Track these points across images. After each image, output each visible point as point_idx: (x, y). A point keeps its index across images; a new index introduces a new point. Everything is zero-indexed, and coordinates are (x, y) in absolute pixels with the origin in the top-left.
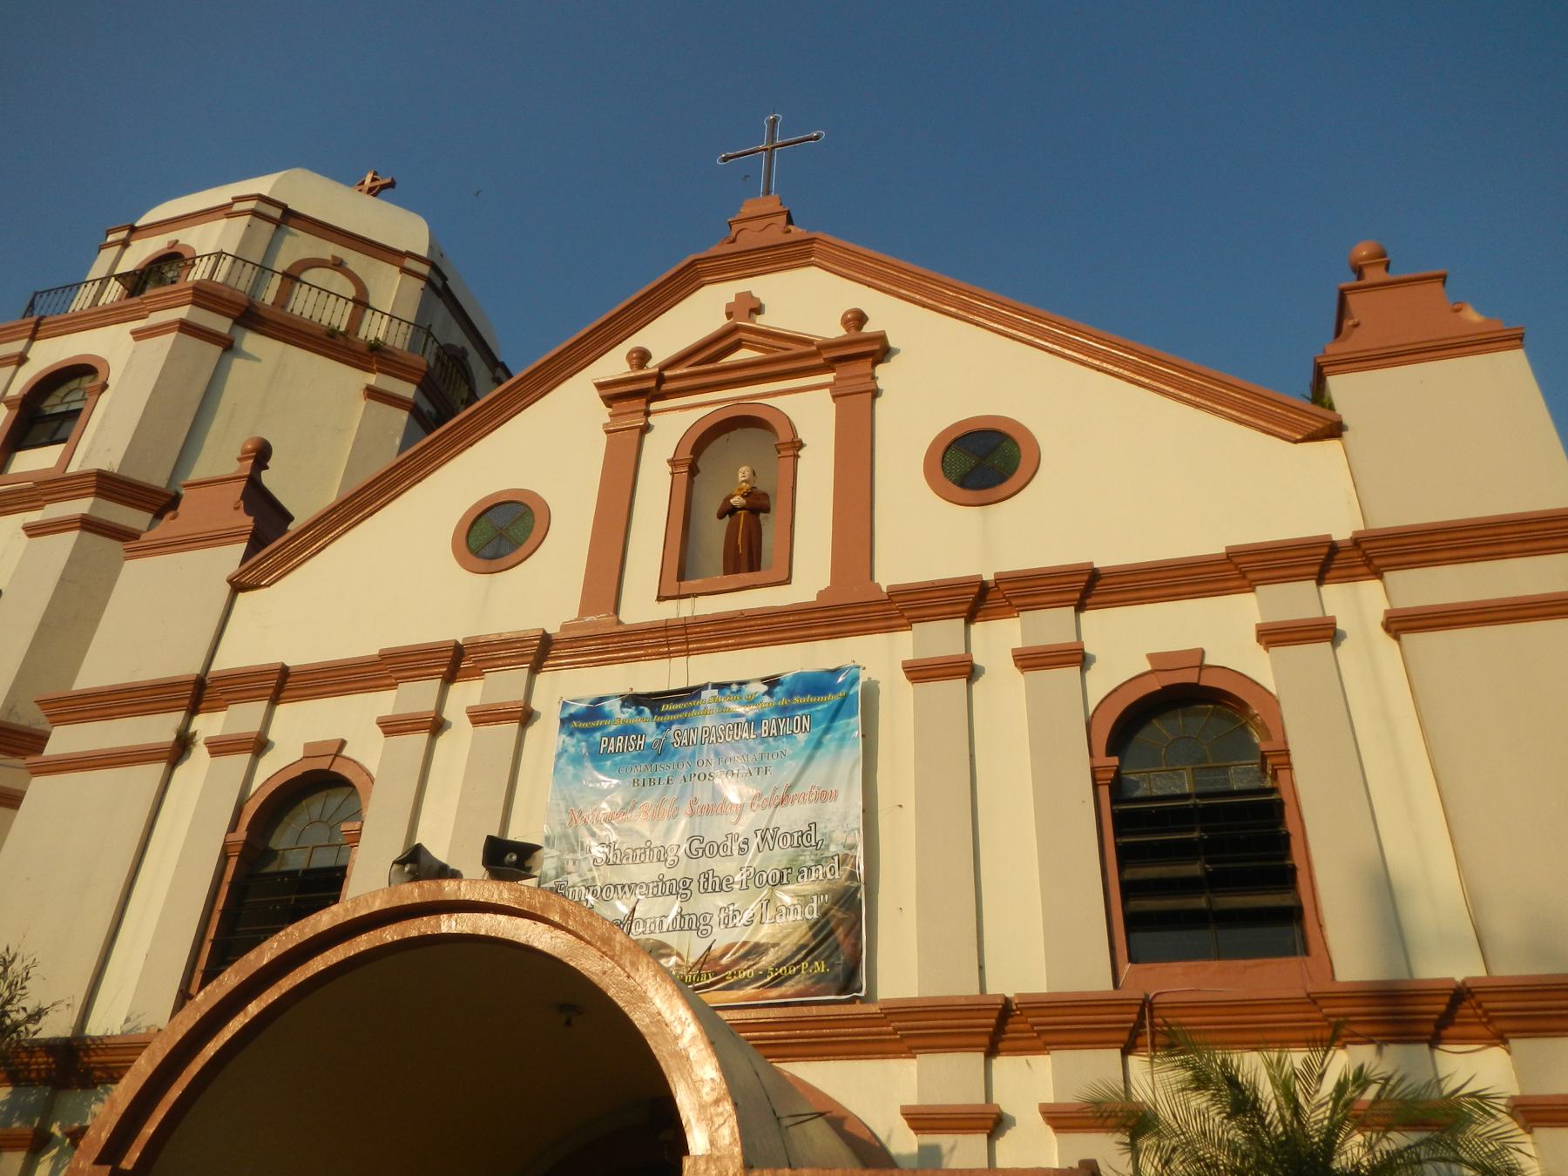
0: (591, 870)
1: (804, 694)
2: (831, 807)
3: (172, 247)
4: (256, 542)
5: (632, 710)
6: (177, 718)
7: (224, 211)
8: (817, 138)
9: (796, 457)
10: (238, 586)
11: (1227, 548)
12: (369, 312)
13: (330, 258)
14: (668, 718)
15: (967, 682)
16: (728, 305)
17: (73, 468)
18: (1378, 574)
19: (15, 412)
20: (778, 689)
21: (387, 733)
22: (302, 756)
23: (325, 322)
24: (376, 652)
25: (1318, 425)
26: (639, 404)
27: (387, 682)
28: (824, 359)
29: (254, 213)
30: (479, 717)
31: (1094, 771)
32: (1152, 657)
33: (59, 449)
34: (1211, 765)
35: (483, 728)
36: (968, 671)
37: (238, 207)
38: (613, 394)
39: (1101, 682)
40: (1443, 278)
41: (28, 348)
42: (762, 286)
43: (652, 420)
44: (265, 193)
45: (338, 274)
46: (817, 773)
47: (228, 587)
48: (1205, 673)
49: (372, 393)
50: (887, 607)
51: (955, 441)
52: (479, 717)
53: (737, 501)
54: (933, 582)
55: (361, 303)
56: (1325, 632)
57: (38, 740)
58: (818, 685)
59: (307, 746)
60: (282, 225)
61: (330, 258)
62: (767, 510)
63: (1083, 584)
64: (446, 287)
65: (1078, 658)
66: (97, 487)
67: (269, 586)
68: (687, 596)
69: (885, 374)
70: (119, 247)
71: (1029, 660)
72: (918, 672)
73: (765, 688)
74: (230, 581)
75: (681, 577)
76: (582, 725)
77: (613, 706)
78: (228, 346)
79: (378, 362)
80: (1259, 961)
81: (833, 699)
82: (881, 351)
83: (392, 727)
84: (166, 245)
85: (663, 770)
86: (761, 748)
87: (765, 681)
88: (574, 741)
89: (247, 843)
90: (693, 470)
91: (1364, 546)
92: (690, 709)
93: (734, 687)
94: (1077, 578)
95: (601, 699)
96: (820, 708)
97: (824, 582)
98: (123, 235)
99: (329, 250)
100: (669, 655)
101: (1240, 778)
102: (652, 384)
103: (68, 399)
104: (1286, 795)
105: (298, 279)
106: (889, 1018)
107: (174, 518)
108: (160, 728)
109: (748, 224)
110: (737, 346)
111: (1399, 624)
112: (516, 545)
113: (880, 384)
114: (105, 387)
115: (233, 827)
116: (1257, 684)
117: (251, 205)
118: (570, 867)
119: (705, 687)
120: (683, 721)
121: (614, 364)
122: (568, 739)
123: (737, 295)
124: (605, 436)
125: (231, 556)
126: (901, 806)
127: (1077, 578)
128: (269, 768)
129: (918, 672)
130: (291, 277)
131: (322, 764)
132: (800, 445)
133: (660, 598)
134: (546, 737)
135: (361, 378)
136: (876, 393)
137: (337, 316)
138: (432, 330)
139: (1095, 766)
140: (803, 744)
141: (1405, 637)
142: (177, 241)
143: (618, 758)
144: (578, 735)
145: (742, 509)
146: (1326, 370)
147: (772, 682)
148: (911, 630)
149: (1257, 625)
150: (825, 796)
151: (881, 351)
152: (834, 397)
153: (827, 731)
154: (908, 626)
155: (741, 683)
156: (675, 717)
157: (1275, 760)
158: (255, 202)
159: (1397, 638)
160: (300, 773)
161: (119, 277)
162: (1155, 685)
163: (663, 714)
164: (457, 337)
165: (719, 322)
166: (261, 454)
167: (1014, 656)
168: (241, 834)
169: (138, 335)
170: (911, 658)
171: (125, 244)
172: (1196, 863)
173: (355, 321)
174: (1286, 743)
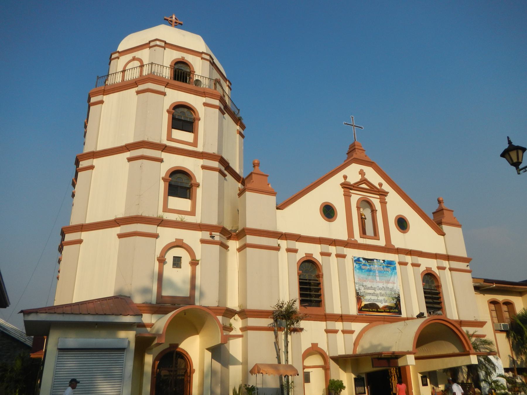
0: (364, 290)
1: (389, 264)
2: (395, 285)
5: (364, 261)
8: (362, 128)
14: (370, 264)
18: (448, 261)
20: (385, 262)
32: (426, 267)
37: (204, 56)
40: (453, 211)
46: (392, 279)
58: (390, 263)
66: (220, 160)
73: (383, 262)
76: (358, 262)
77: (361, 259)
79: (240, 123)
81: (393, 266)
83: (322, 254)
85: (371, 273)
86: (385, 273)
87: (383, 260)
88: (357, 265)
92: (373, 263)
93: (378, 260)
95: (359, 258)
96: (391, 267)
100: (364, 250)
109: (359, 150)
111: (451, 269)
114: (199, 119)
118: (360, 289)
119: (374, 259)
120: (372, 265)
133: (361, 237)
134: (349, 262)
140: (390, 273)
143: (365, 270)
146: (443, 224)
147: (384, 261)
150: (394, 283)
153: (393, 272)
155: (379, 260)
156: (371, 264)
162: (426, 272)
163: (369, 263)
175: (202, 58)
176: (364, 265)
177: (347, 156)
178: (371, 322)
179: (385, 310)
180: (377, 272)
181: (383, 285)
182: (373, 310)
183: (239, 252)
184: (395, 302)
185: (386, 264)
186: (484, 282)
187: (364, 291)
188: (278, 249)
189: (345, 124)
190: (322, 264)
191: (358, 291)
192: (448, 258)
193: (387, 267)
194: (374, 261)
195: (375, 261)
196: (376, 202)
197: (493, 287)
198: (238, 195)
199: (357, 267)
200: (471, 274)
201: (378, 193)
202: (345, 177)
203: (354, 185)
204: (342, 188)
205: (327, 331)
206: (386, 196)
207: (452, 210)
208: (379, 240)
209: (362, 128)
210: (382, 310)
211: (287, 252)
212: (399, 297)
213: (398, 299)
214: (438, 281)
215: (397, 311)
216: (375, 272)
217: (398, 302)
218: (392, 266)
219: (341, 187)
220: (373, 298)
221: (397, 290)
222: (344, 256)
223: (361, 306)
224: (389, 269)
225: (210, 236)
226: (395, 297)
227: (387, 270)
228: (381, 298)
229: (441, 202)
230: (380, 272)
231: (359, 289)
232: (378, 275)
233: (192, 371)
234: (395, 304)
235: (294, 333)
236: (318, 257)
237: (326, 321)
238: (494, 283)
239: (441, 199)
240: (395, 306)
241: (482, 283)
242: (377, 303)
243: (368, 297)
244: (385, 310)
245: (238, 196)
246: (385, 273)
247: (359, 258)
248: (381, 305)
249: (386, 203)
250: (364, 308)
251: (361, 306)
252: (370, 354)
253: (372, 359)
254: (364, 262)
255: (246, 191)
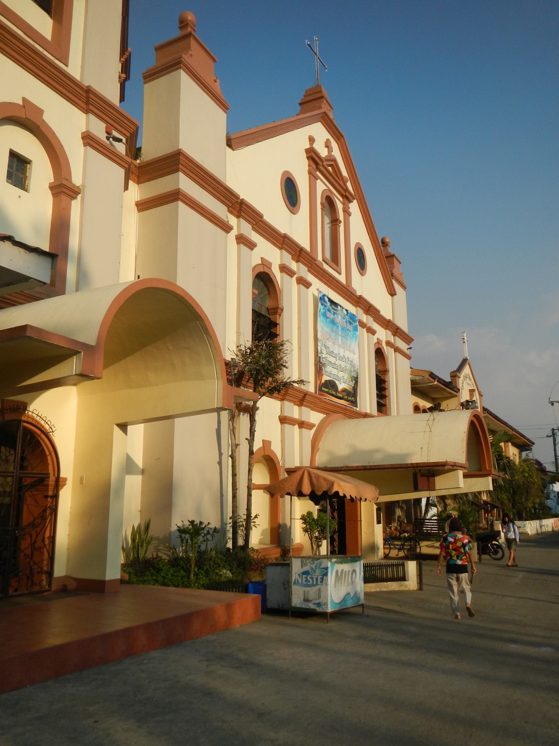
14: (334, 311)
40: (400, 263)
58: (352, 317)
83: (284, 269)
91: (398, 330)
110: (331, 165)
118: (323, 351)
122: (321, 306)
141: (397, 353)
144: (323, 306)
147: (347, 310)
155: (343, 308)
156: (335, 312)
163: (333, 308)
176: (329, 310)
177: (299, 107)
178: (329, 412)
179: (343, 396)
180: (340, 329)
181: (344, 352)
182: (333, 393)
183: (140, 210)
184: (353, 386)
185: (349, 317)
186: (430, 376)
187: (326, 357)
188: (227, 228)
190: (282, 287)
191: (320, 355)
192: (396, 331)
193: (350, 323)
194: (337, 307)
195: (339, 307)
196: (340, 206)
197: (434, 384)
198: (145, 78)
199: (322, 310)
200: (410, 363)
201: (344, 194)
202: (312, 140)
203: (324, 160)
204: (308, 158)
205: (283, 420)
206: (350, 202)
207: (401, 261)
208: (340, 274)
210: (340, 395)
211: (238, 243)
212: (357, 378)
213: (356, 380)
214: (385, 363)
215: (354, 400)
216: (338, 327)
217: (356, 386)
218: (354, 323)
219: (305, 155)
220: (335, 372)
221: (356, 365)
222: (308, 285)
223: (321, 383)
224: (350, 328)
225: (107, 135)
226: (354, 377)
227: (350, 329)
228: (341, 374)
229: (387, 245)
230: (343, 329)
231: (321, 353)
232: (340, 333)
233: (59, 483)
234: (354, 387)
235: (243, 415)
237: (282, 400)
238: (436, 380)
239: (387, 240)
240: (353, 392)
241: (427, 376)
242: (337, 382)
243: (329, 369)
244: (343, 396)
245: (143, 80)
246: (347, 332)
247: (324, 295)
248: (341, 386)
249: (350, 214)
250: (325, 387)
251: (321, 383)
252: (410, 466)
253: (415, 476)
254: (329, 304)
255: (180, 68)
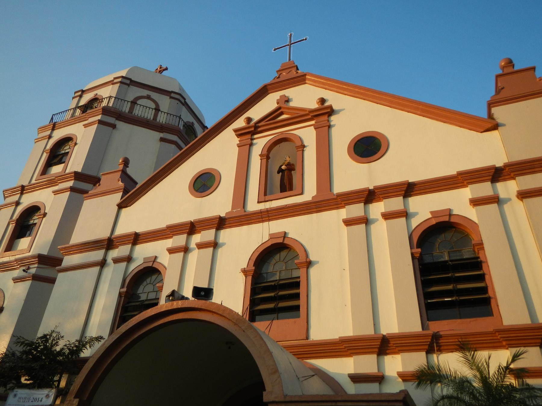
3: (96, 95)
4: (125, 191)
6: (102, 252)
7: (112, 83)
8: (306, 39)
9: (303, 151)
10: (121, 206)
11: (457, 172)
12: (160, 112)
13: (146, 96)
15: (366, 225)
16: (277, 100)
17: (67, 171)
19: (49, 154)
21: (170, 253)
22: (143, 262)
23: (145, 117)
24: (165, 226)
25: (490, 126)
26: (249, 136)
27: (169, 236)
28: (311, 116)
29: (121, 82)
30: (200, 246)
31: (412, 254)
32: (432, 213)
33: (63, 165)
34: (455, 250)
35: (201, 250)
36: (365, 221)
38: (239, 133)
39: (415, 222)
41: (51, 133)
42: (288, 92)
43: (255, 141)
44: (124, 75)
45: (149, 100)
47: (117, 207)
48: (452, 217)
49: (162, 140)
50: (336, 200)
51: (358, 141)
52: (200, 246)
53: (283, 167)
54: (352, 191)
55: (157, 110)
56: (495, 200)
57: (59, 261)
59: (144, 259)
60: (130, 86)
61: (146, 96)
62: (294, 170)
63: (405, 188)
64: (185, 102)
65: (405, 214)
67: (130, 206)
68: (268, 201)
69: (334, 119)
70: (78, 98)
71: (387, 216)
72: (348, 222)
74: (118, 205)
75: (265, 194)
78: (114, 126)
80: (475, 319)
82: (331, 112)
83: (172, 251)
84: (93, 95)
89: (126, 292)
90: (268, 158)
94: (403, 186)
97: (314, 193)
98: (80, 93)
99: (145, 92)
100: (263, 221)
101: (467, 254)
102: (253, 129)
103: (65, 149)
104: (482, 259)
105: (136, 103)
106: (343, 343)
107: (99, 185)
108: (97, 255)
110: (282, 114)
111: (523, 195)
112: (209, 188)
113: (332, 123)
115: (122, 286)
116: (471, 220)
117: (120, 80)
121: (240, 123)
123: (280, 96)
124: (238, 148)
125: (117, 197)
126: (344, 269)
127: (403, 186)
128: (134, 266)
129: (348, 222)
130: (134, 103)
131: (150, 264)
132: (304, 146)
133: (258, 202)
135: (158, 135)
136: (329, 127)
137: (149, 115)
138: (181, 117)
139: (413, 252)
142: (97, 94)
145: (286, 170)
148: (345, 208)
149: (470, 199)
151: (331, 112)
152: (315, 129)
154: (343, 207)
157: (478, 247)
158: (121, 79)
159: (522, 201)
160: (143, 268)
161: (79, 107)
162: (434, 222)
164: (190, 119)
165: (275, 106)
166: (126, 162)
167: (382, 215)
168: (125, 290)
169: (86, 126)
170: (346, 218)
171: (81, 96)
172: (451, 285)
173: (156, 116)
174: (482, 240)
175: (113, 84)
189: (275, 50)
201: (310, 117)
209: (306, 39)
236: (165, 259)
